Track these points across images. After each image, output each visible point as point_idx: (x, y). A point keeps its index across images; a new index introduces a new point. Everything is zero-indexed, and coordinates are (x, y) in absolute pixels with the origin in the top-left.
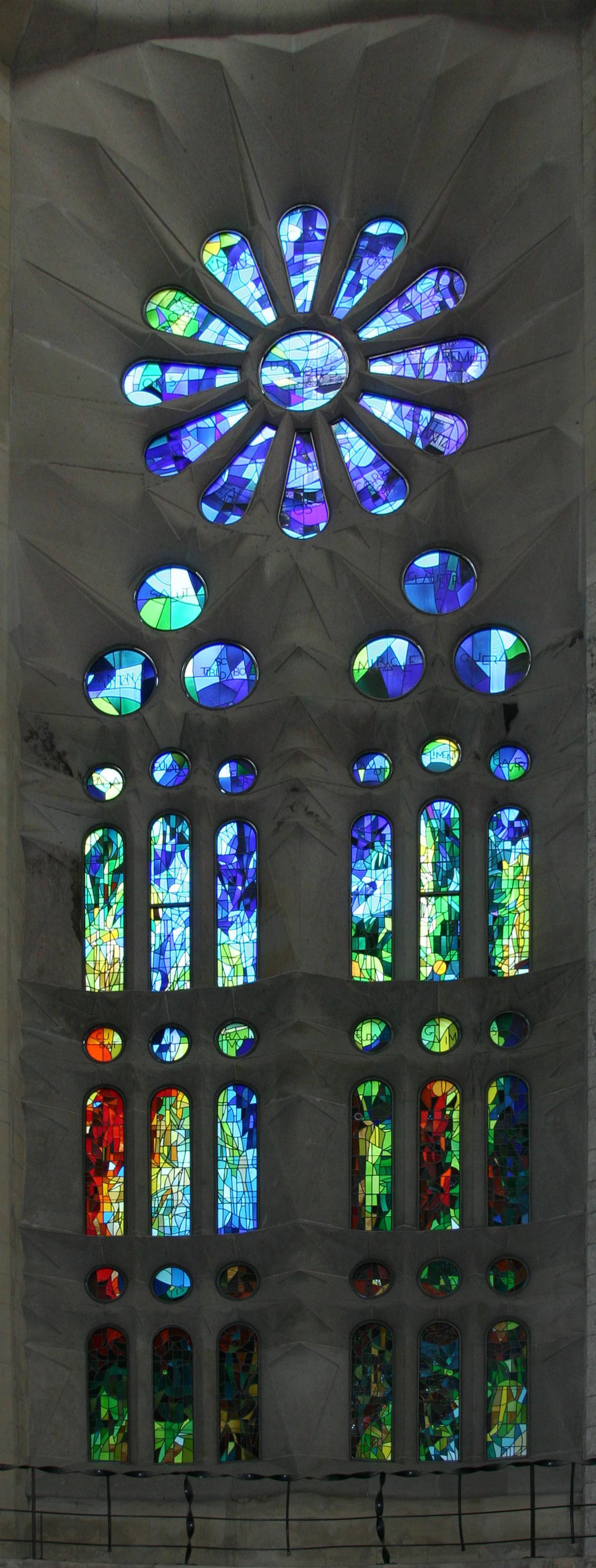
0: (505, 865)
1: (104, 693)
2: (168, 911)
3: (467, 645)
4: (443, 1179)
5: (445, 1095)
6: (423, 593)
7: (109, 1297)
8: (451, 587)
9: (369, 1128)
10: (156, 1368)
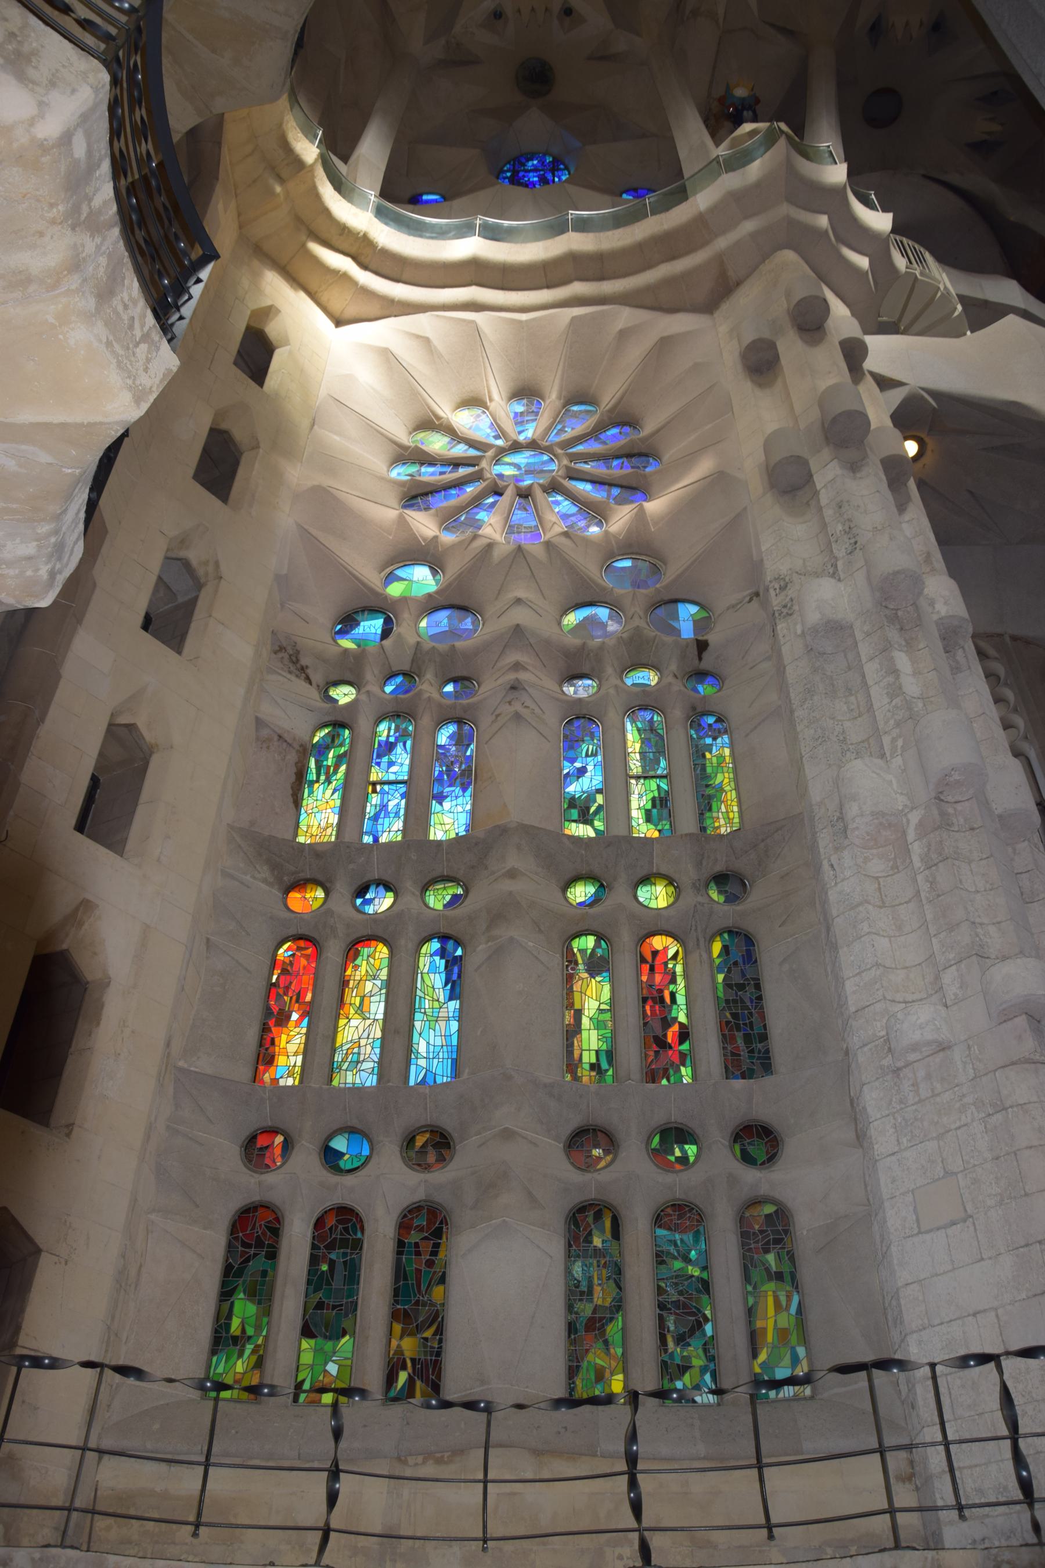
0: (708, 755)
1: (349, 636)
2: (386, 787)
4: (670, 1035)
5: (666, 949)
7: (268, 1166)
9: (585, 980)
10: (314, 1260)
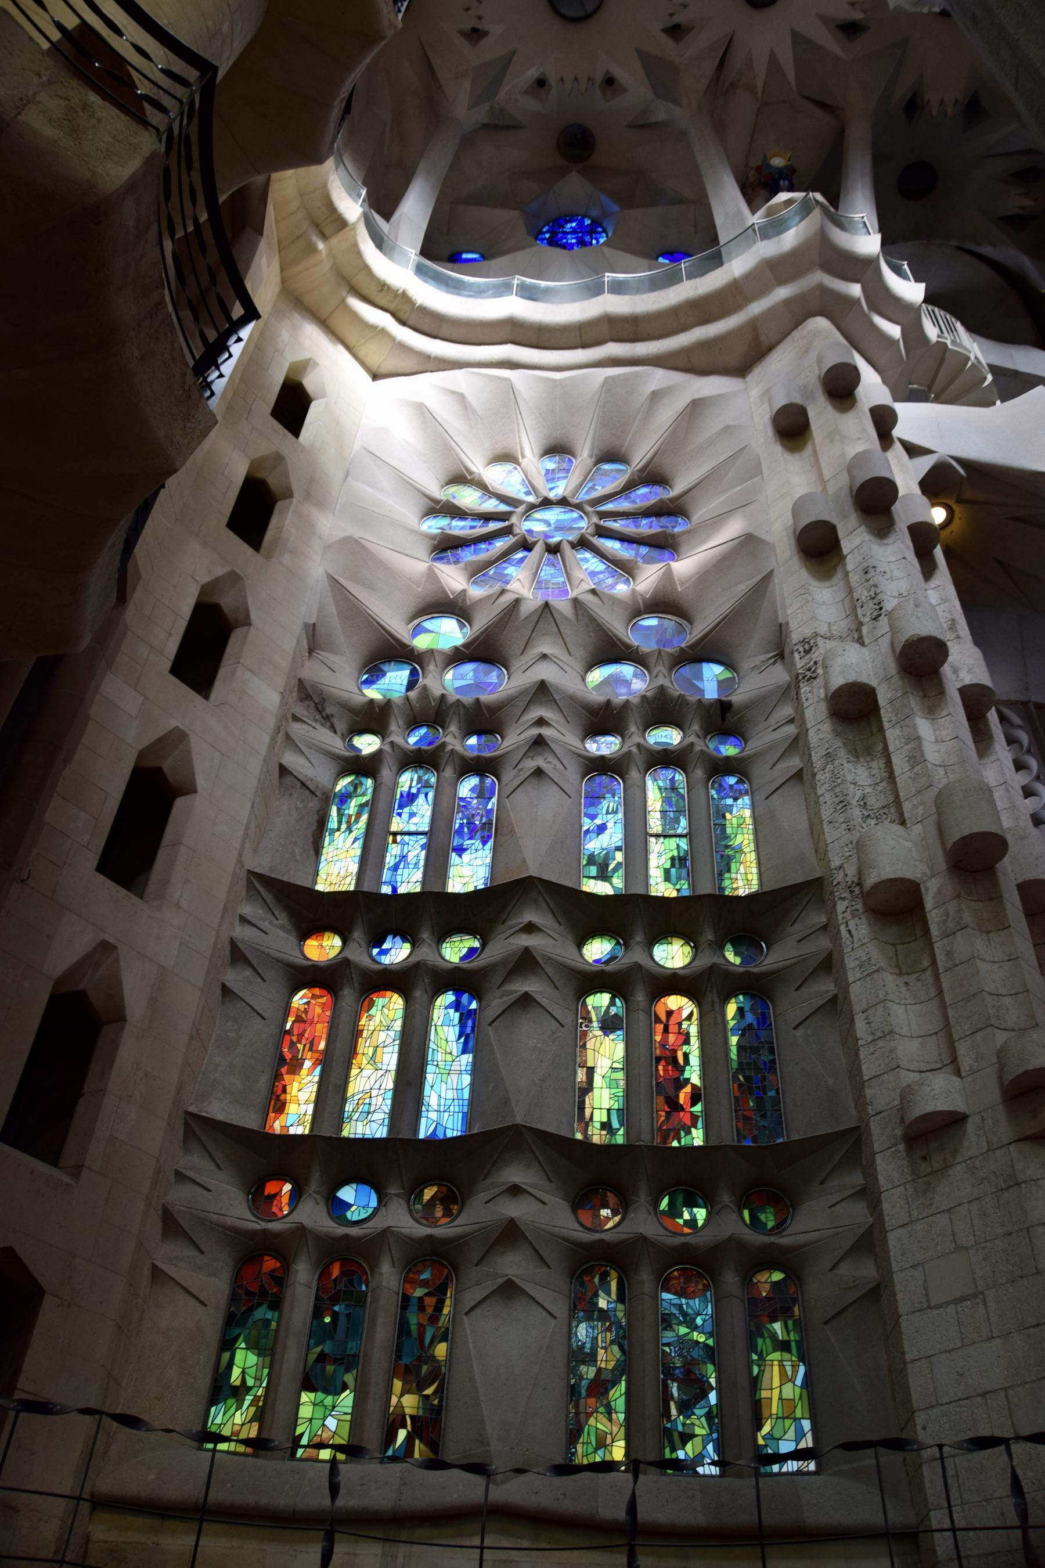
0: (728, 816)
1: (374, 686)
2: (406, 838)
5: (680, 1009)
7: (274, 1214)
10: (318, 1314)
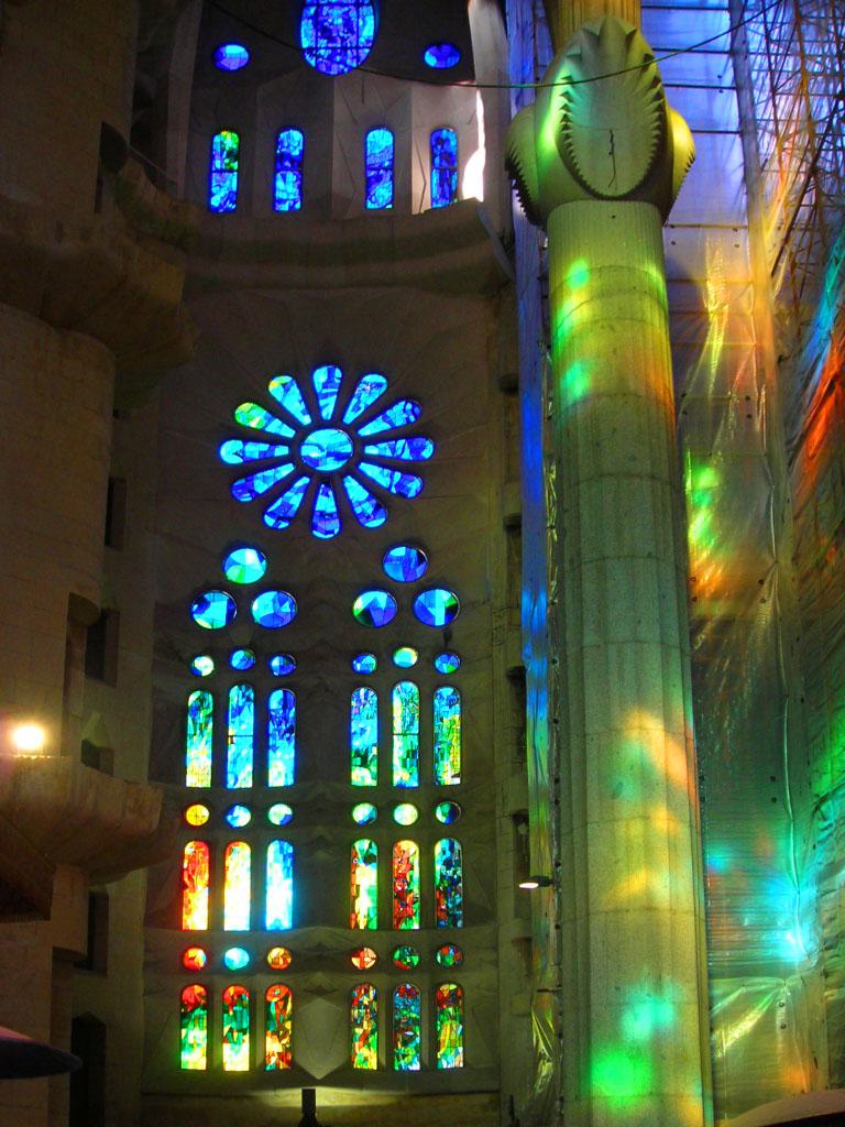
3: (421, 598)
6: (396, 570)
8: (412, 566)
